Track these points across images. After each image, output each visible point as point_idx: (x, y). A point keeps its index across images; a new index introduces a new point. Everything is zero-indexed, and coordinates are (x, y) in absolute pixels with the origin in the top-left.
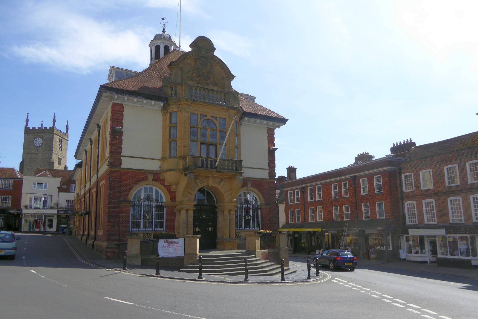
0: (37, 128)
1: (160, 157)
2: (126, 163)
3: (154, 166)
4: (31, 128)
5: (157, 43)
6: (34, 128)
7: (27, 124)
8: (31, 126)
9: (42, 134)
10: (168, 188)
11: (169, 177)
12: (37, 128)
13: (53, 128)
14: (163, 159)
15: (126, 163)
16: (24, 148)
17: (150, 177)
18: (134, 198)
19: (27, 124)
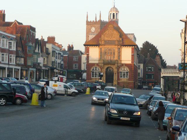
0: (92, 21)
1: (98, 60)
2: (90, 62)
3: (97, 62)
4: (89, 21)
5: (111, 13)
6: (91, 21)
7: (87, 19)
8: (89, 20)
9: (95, 25)
10: (100, 67)
11: (100, 64)
12: (92, 21)
13: (100, 21)
14: (99, 60)
15: (90, 62)
16: (86, 34)
17: (96, 65)
18: (93, 70)
19: (87, 19)
